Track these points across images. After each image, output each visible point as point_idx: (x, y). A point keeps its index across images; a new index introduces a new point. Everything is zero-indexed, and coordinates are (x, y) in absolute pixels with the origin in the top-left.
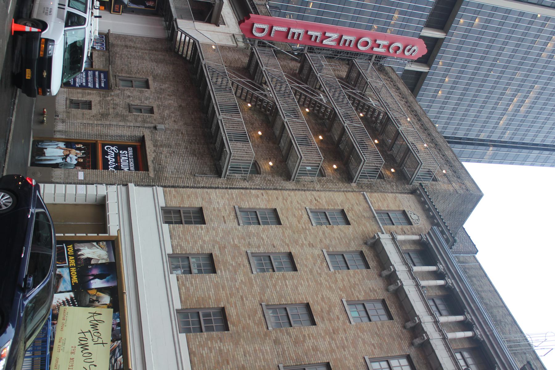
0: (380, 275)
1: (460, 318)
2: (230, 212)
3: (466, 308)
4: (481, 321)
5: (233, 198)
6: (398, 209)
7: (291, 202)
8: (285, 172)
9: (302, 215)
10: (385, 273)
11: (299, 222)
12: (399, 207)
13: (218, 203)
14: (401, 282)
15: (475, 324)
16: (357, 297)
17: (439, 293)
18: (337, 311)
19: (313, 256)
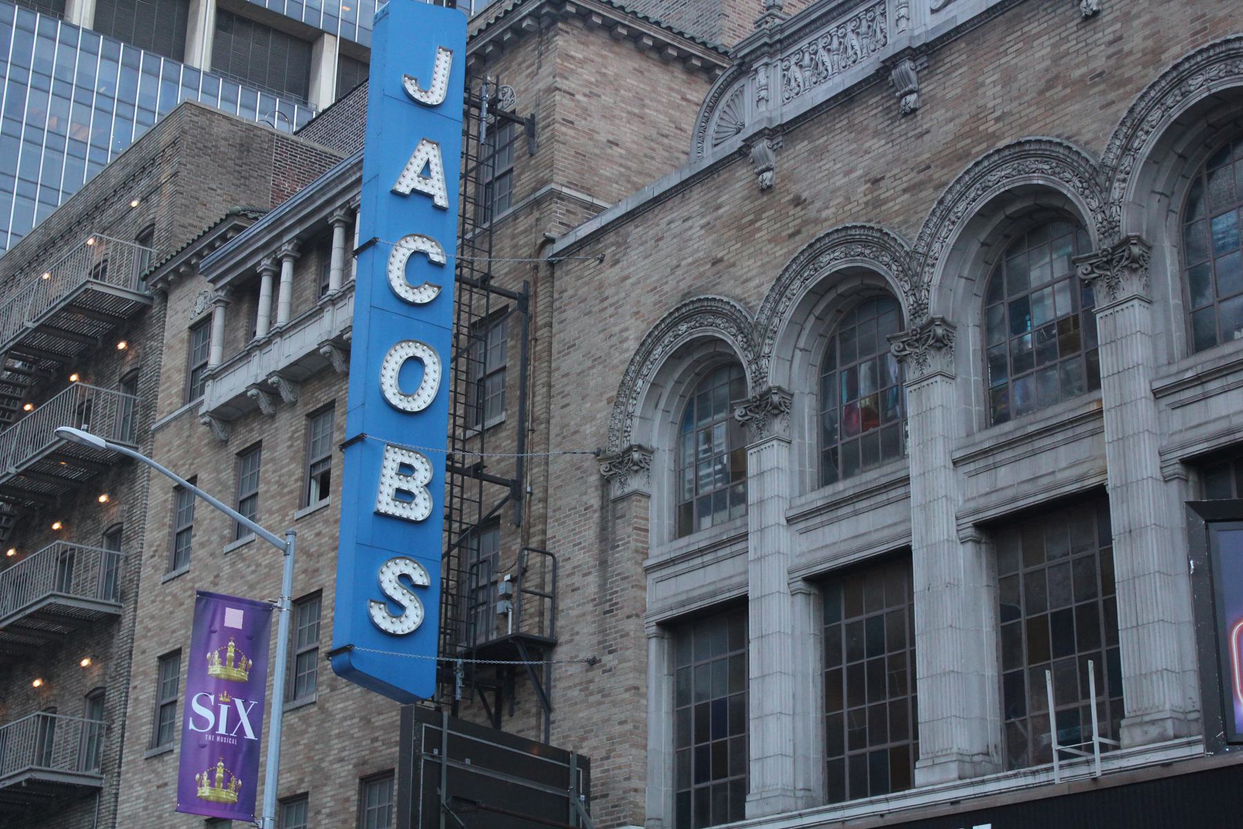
0: (272, 417)
1: (338, 235)
2: (154, 771)
3: (326, 218)
4: (340, 187)
5: (134, 761)
6: (185, 346)
7: (153, 618)
8: (98, 629)
9: (171, 593)
10: (264, 405)
11: (182, 604)
12: (182, 341)
13: (138, 798)
14: (270, 375)
15: (348, 202)
16: (296, 481)
17: (311, 274)
18: (309, 535)
19: (232, 578)
